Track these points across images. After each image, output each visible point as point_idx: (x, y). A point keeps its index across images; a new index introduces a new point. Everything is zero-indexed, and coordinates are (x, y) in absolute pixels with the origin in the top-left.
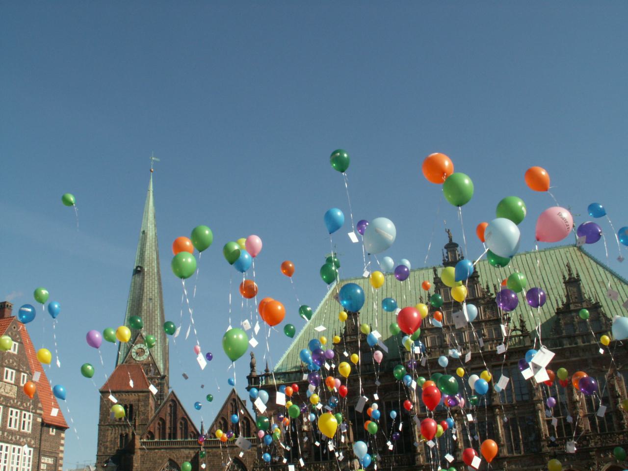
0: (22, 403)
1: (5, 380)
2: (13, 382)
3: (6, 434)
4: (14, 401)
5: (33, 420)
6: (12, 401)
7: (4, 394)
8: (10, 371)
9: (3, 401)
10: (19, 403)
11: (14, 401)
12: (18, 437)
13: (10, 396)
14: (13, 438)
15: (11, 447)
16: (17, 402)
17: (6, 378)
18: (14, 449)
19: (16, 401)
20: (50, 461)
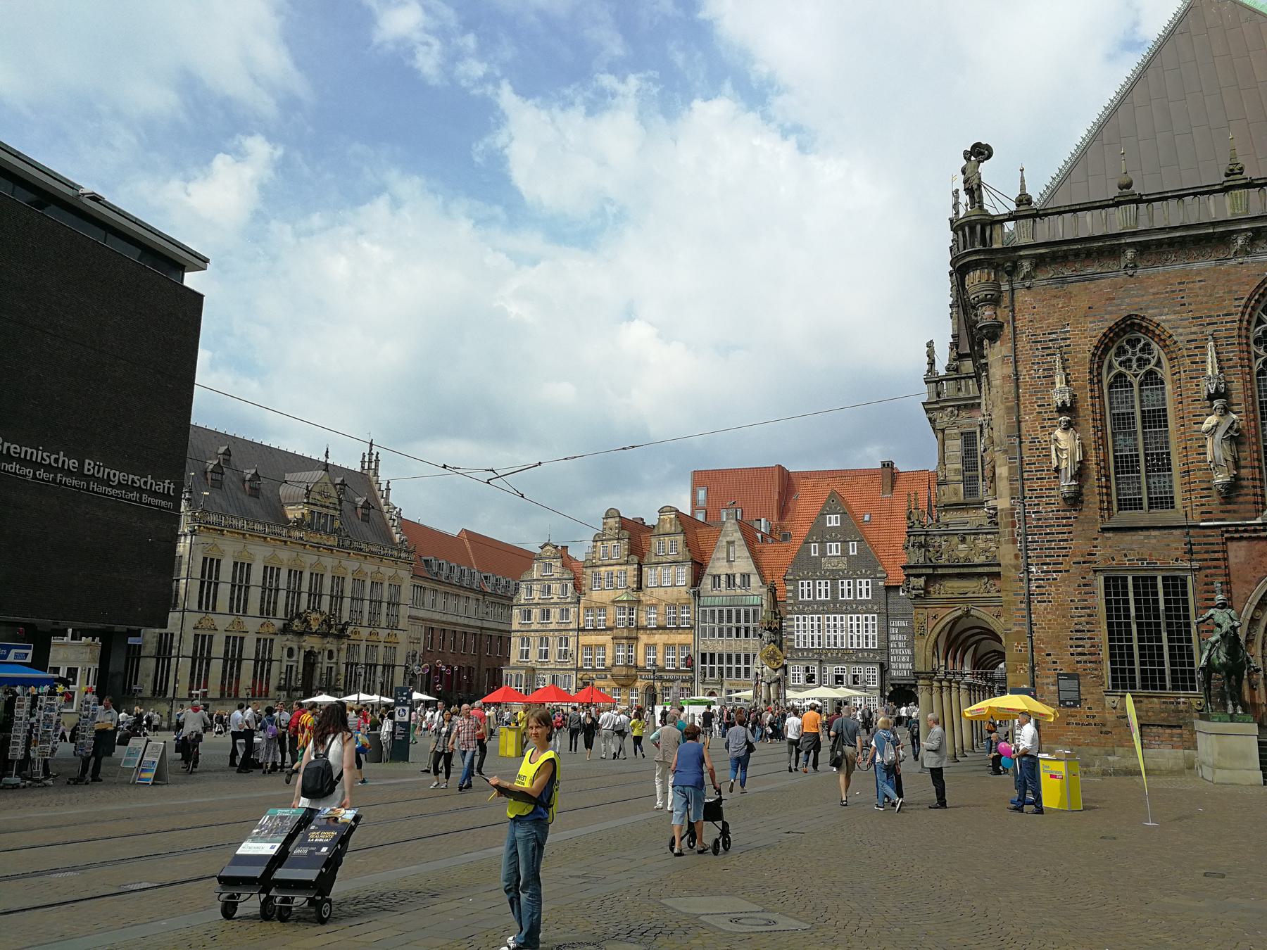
0: (855, 572)
1: (829, 554)
2: (839, 554)
3: (838, 605)
4: (843, 572)
5: (872, 585)
6: (841, 573)
7: (831, 568)
8: (834, 545)
9: (829, 575)
10: (851, 572)
11: (843, 572)
12: (854, 606)
13: (838, 568)
14: (849, 608)
15: (847, 617)
16: (848, 572)
17: (831, 552)
18: (851, 618)
19: (846, 572)
20: (904, 624)
